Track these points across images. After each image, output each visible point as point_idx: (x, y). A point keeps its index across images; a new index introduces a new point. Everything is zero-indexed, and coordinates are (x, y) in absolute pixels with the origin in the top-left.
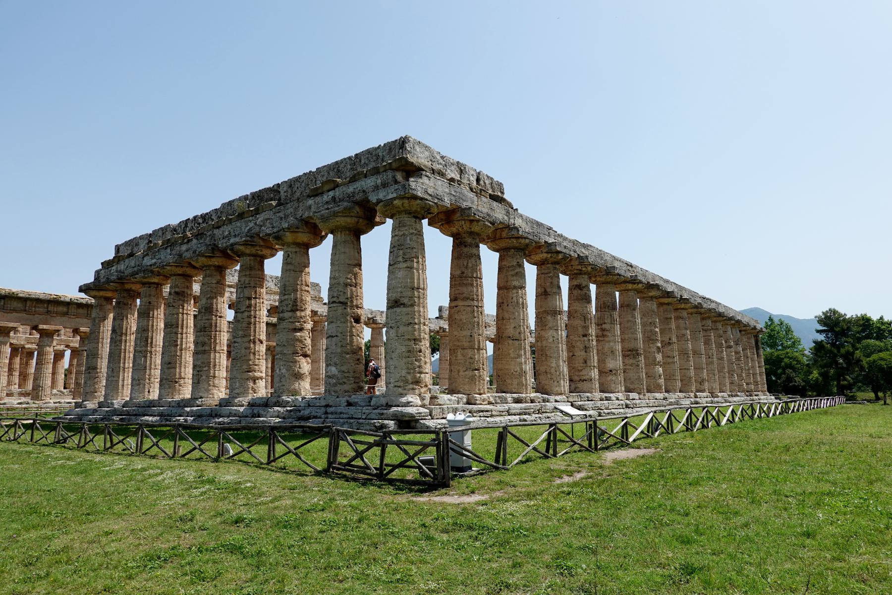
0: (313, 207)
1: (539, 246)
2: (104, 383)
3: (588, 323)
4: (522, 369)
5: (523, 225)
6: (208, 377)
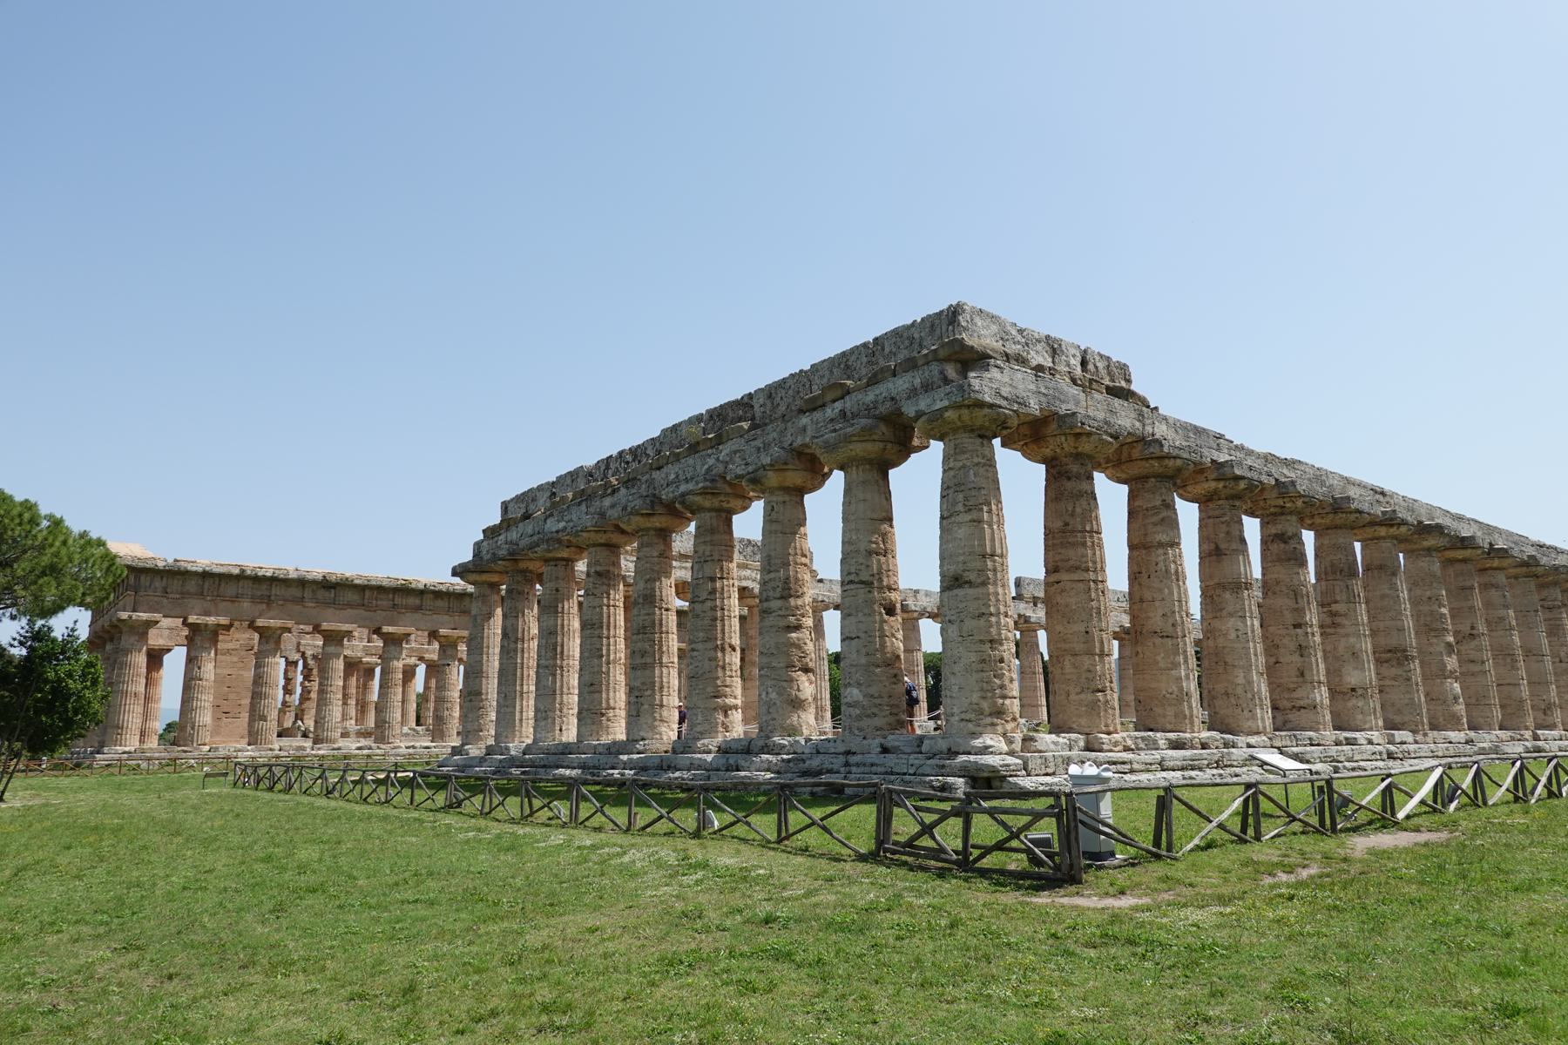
1: (1200, 470)
2: (493, 716)
3: (1303, 602)
4: (1181, 689)
5: (1170, 434)
6: (652, 705)
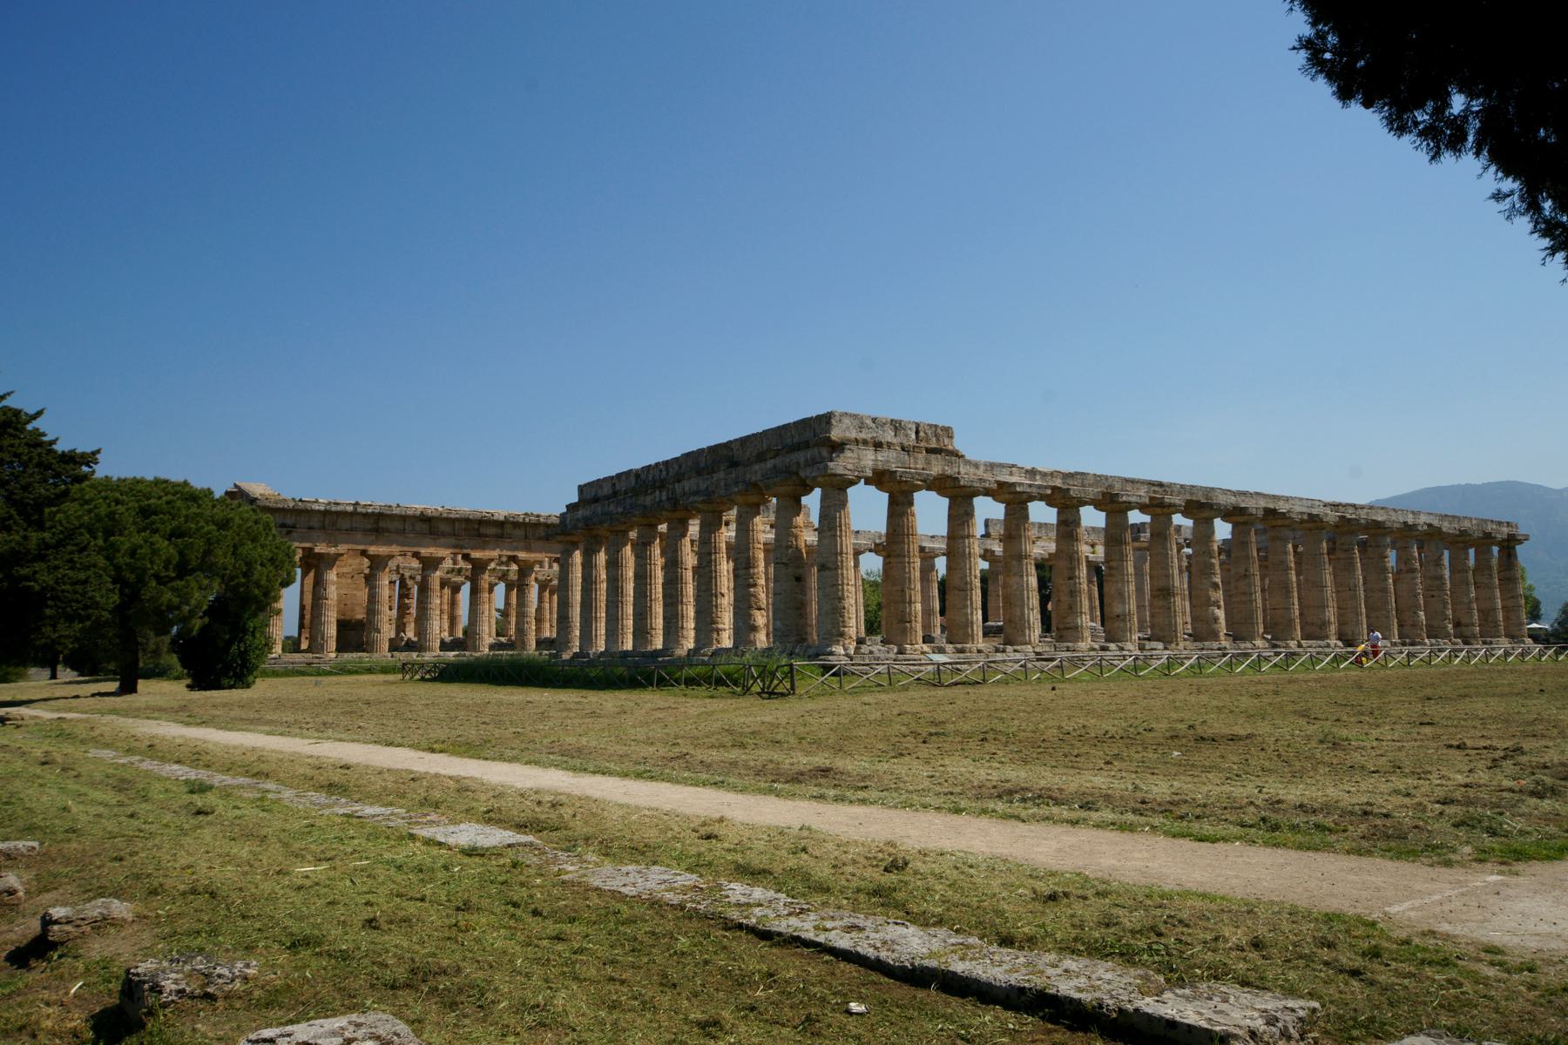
0: (757, 472)
